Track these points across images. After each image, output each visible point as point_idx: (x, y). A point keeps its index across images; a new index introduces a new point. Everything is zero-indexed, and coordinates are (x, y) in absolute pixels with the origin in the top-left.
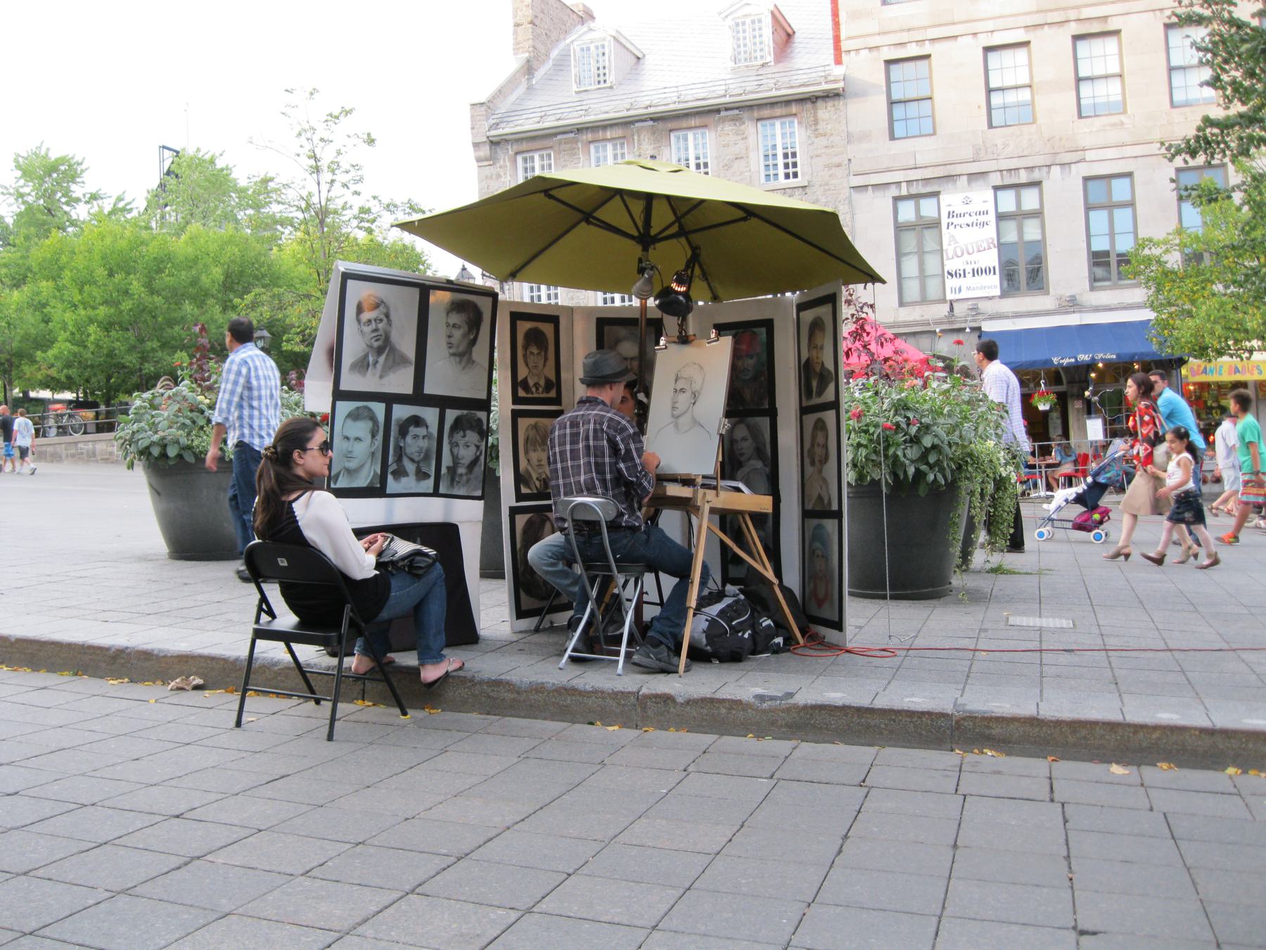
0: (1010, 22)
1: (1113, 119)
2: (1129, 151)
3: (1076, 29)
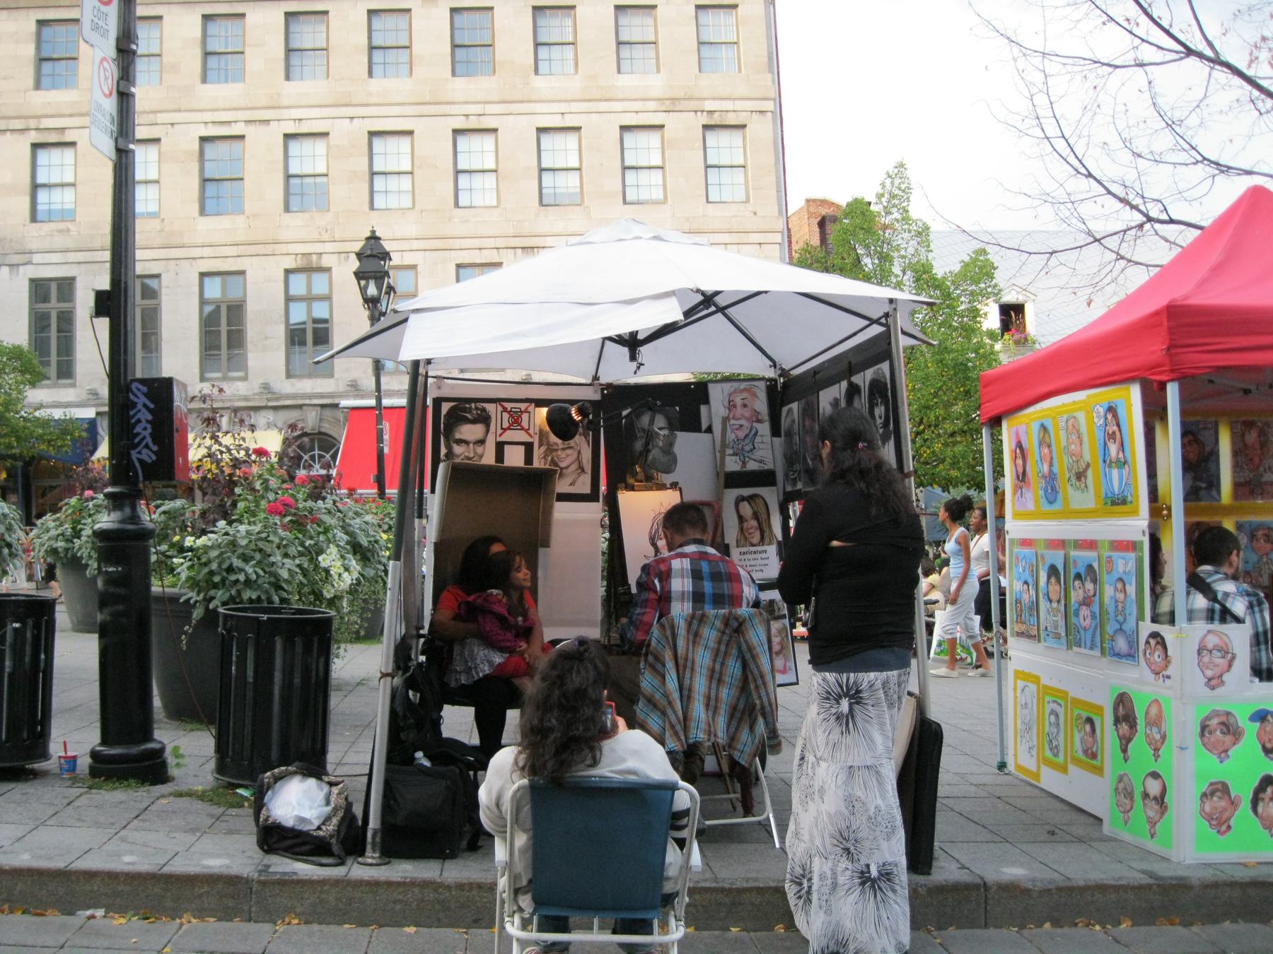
1: (62, 226)
2: (72, 257)
3: (34, 137)
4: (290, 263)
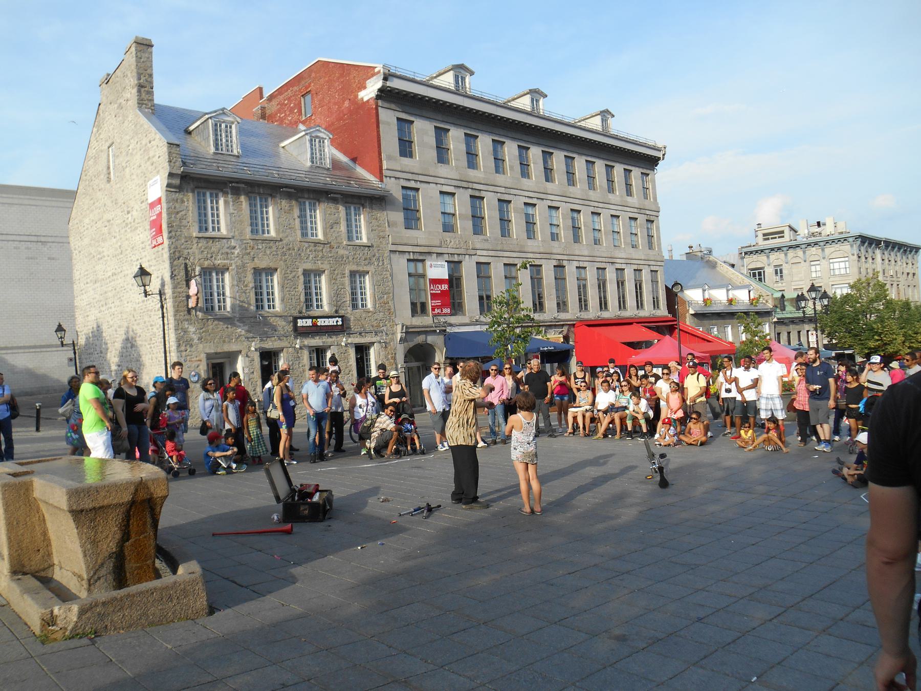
0: (449, 182)
3: (470, 192)
4: (555, 263)
